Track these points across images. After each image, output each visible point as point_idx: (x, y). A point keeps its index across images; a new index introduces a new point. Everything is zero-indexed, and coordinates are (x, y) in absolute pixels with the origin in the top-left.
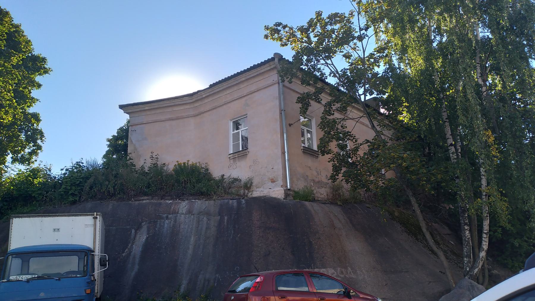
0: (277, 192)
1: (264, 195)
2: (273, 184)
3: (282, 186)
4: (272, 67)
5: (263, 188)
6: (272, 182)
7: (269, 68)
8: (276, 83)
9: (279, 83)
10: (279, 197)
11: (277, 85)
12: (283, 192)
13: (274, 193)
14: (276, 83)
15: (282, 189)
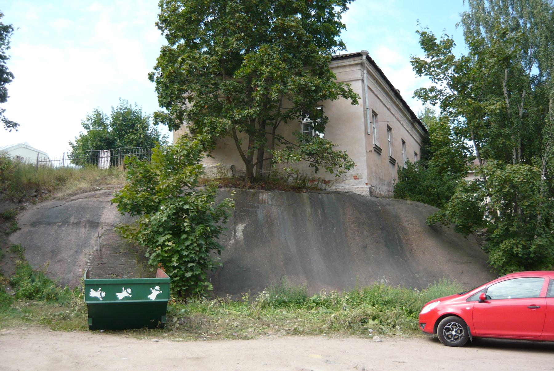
0: (362, 189)
1: (346, 191)
2: (356, 181)
3: (367, 184)
4: (356, 62)
5: (345, 183)
6: (355, 179)
7: (352, 63)
8: (360, 80)
9: (363, 81)
10: (364, 194)
11: (361, 81)
12: (368, 190)
13: (358, 189)
14: (360, 80)
15: (367, 186)
